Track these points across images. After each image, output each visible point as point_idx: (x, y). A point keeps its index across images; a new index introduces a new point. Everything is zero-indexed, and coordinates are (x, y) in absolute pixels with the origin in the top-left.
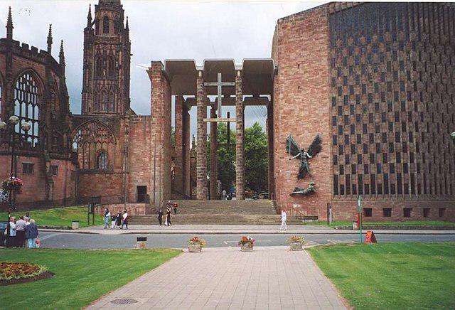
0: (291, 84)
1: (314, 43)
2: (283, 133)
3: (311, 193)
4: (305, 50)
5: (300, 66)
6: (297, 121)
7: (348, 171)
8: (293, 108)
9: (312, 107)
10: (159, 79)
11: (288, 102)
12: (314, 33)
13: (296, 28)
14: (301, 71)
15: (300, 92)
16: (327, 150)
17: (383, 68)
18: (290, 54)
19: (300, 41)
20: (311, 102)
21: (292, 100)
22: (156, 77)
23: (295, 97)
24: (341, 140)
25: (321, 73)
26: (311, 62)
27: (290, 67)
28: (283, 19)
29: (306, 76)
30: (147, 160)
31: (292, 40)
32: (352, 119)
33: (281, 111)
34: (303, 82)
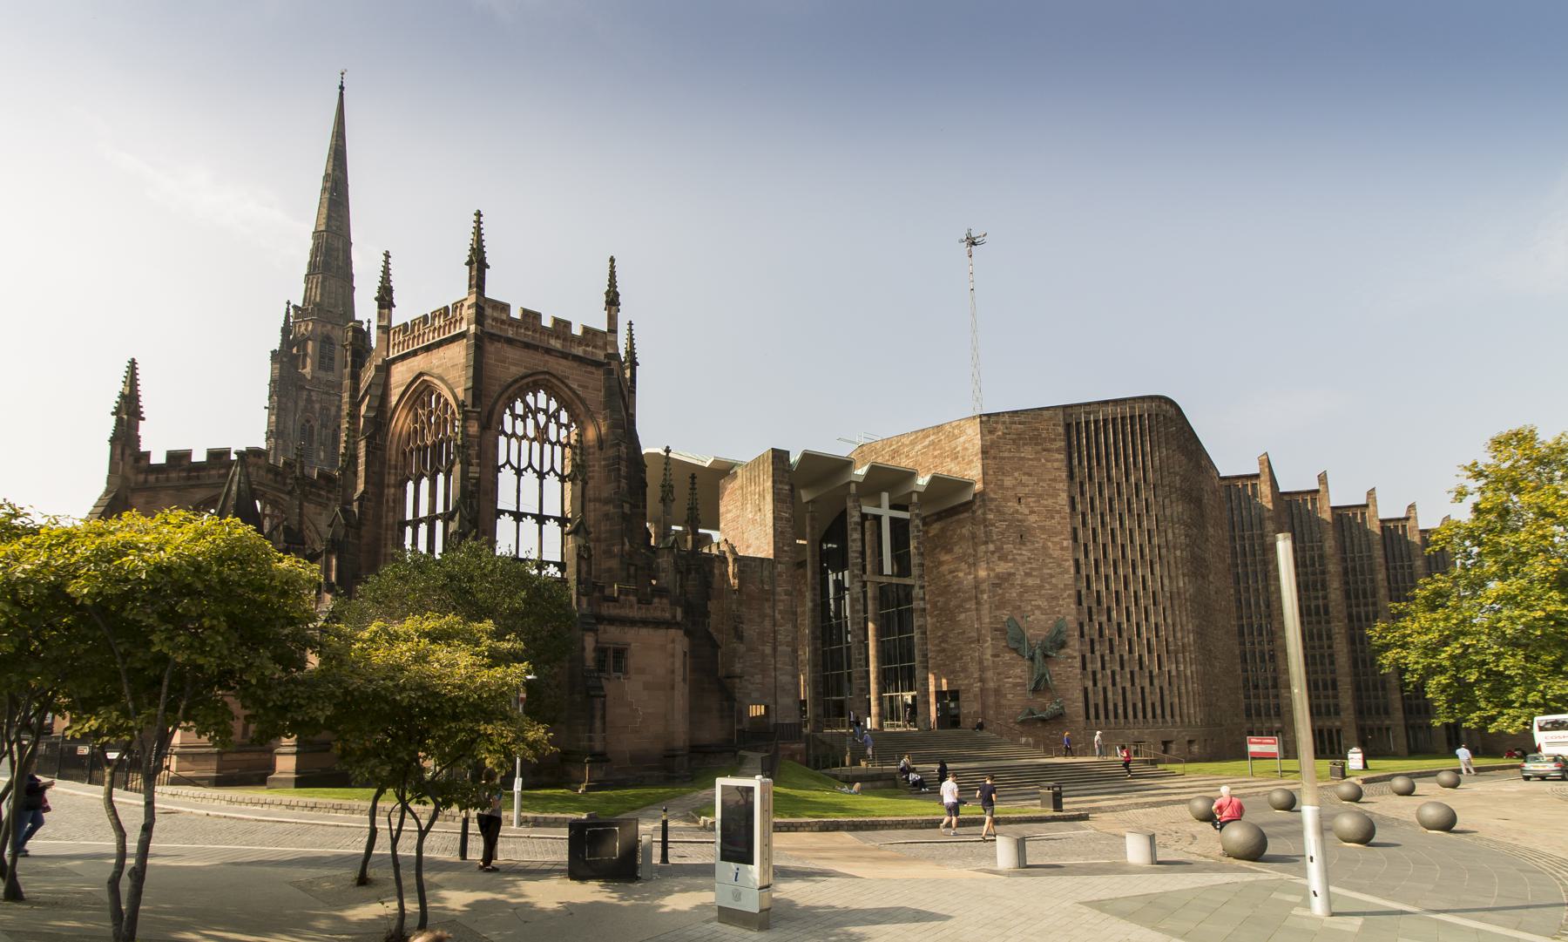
1: (1044, 465)
2: (998, 613)
3: (1058, 718)
4: (1030, 475)
6: (1021, 595)
8: (1013, 571)
11: (1003, 558)
12: (1045, 450)
13: (1014, 437)
14: (1027, 512)
16: (1075, 647)
18: (1006, 479)
19: (1022, 459)
20: (1044, 565)
21: (1010, 557)
23: (1015, 551)
24: (1092, 631)
25: (1057, 516)
26: (1040, 496)
27: (1006, 500)
28: (989, 415)
29: (1033, 518)
30: (768, 650)
31: (1006, 454)
34: (1028, 529)
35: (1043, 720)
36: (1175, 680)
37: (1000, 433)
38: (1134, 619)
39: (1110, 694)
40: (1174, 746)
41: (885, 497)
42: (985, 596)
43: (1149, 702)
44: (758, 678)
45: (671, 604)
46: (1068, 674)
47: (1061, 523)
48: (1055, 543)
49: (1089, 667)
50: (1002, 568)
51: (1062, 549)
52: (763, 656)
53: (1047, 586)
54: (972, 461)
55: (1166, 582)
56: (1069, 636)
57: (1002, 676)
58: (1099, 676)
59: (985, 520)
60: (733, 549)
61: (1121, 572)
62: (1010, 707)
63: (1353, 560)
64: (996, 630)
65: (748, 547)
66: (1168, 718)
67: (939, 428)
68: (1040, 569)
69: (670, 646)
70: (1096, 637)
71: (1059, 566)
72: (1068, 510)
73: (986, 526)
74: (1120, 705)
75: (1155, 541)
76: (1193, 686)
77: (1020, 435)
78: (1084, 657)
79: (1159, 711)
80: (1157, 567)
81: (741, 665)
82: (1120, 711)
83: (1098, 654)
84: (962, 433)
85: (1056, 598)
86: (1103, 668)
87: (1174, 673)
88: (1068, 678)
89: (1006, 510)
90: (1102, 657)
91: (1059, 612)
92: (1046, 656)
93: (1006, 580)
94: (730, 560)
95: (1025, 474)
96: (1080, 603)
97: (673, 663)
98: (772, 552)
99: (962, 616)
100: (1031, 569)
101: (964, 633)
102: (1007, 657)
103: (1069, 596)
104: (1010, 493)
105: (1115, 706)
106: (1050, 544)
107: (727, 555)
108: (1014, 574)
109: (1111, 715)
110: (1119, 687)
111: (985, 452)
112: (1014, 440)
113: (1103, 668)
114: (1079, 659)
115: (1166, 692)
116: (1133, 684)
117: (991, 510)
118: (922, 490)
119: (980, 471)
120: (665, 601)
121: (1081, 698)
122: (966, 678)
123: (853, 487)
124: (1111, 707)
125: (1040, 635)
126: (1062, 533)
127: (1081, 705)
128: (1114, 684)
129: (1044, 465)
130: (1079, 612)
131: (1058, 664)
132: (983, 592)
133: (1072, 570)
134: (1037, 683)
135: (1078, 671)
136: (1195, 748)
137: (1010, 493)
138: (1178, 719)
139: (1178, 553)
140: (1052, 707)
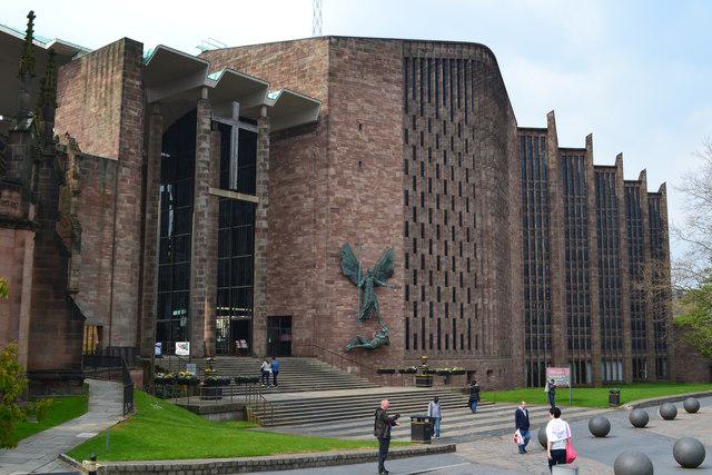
0: (347, 155)
1: (383, 95)
2: (334, 238)
4: (371, 102)
5: (364, 128)
6: (356, 222)
7: (423, 312)
8: (350, 197)
9: (379, 200)
10: (138, 83)
12: (385, 80)
13: (359, 63)
14: (366, 138)
15: (361, 170)
16: (400, 276)
17: (467, 163)
21: (349, 183)
22: (133, 77)
24: (415, 261)
25: (392, 147)
26: (379, 126)
27: (347, 124)
28: (338, 38)
29: (371, 146)
30: (106, 263)
31: (351, 79)
32: (430, 232)
33: (332, 199)
34: (367, 155)
35: (369, 350)
36: (480, 313)
37: (347, 57)
38: (451, 253)
39: (427, 325)
40: (476, 377)
41: (236, 105)
42: (324, 221)
43: (458, 334)
44: (92, 295)
45: (24, 199)
46: (392, 301)
47: (396, 153)
48: (389, 173)
49: (412, 298)
50: (340, 194)
51: (395, 179)
52: (100, 268)
53: (380, 216)
54: (318, 82)
55: (478, 220)
56: (396, 266)
57: (335, 304)
58: (419, 307)
59: (328, 143)
60: (74, 145)
61: (442, 206)
62: (341, 335)
63: (604, 212)
64: (332, 256)
65: (88, 145)
66: (473, 349)
67: (288, 44)
68: (374, 198)
69: (18, 250)
70: (419, 268)
71: (391, 196)
72: (402, 141)
73: (328, 149)
74: (435, 335)
75: (471, 180)
76: (494, 320)
77: (365, 62)
78: (407, 287)
79: (466, 343)
80: (471, 204)
81: (76, 279)
82: (435, 342)
83: (419, 284)
84: (311, 51)
85: (386, 228)
86: (423, 300)
87: (479, 307)
88: (394, 308)
89: (348, 134)
90: (423, 288)
91: (389, 242)
92: (376, 285)
93: (344, 205)
94: (72, 157)
95: (367, 101)
96: (407, 235)
97: (22, 271)
98: (116, 153)
99: (300, 240)
100: (367, 196)
101: (300, 257)
102: (341, 283)
103: (398, 226)
104: (352, 119)
105: (431, 335)
106: (385, 174)
107: (68, 151)
108: (351, 200)
109: (427, 345)
110: (435, 318)
111: (332, 74)
112: (359, 67)
113: (423, 300)
114: (403, 289)
115: (473, 325)
116: (447, 317)
117: (334, 133)
118: (271, 104)
119: (326, 92)
120: (15, 194)
121: (404, 329)
122: (300, 303)
123: (205, 93)
124: (427, 337)
125: (371, 263)
126: (396, 164)
127: (403, 335)
128: (431, 316)
129: (383, 95)
130: (406, 244)
131: (384, 293)
132: (321, 216)
133: (402, 201)
134: (367, 312)
135: (402, 301)
136: (493, 377)
137: (352, 119)
138: (481, 350)
139: (489, 193)
140: (377, 339)
